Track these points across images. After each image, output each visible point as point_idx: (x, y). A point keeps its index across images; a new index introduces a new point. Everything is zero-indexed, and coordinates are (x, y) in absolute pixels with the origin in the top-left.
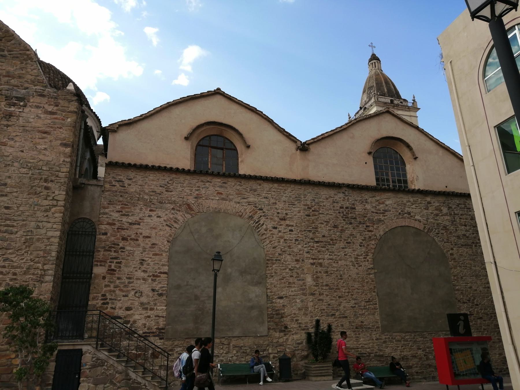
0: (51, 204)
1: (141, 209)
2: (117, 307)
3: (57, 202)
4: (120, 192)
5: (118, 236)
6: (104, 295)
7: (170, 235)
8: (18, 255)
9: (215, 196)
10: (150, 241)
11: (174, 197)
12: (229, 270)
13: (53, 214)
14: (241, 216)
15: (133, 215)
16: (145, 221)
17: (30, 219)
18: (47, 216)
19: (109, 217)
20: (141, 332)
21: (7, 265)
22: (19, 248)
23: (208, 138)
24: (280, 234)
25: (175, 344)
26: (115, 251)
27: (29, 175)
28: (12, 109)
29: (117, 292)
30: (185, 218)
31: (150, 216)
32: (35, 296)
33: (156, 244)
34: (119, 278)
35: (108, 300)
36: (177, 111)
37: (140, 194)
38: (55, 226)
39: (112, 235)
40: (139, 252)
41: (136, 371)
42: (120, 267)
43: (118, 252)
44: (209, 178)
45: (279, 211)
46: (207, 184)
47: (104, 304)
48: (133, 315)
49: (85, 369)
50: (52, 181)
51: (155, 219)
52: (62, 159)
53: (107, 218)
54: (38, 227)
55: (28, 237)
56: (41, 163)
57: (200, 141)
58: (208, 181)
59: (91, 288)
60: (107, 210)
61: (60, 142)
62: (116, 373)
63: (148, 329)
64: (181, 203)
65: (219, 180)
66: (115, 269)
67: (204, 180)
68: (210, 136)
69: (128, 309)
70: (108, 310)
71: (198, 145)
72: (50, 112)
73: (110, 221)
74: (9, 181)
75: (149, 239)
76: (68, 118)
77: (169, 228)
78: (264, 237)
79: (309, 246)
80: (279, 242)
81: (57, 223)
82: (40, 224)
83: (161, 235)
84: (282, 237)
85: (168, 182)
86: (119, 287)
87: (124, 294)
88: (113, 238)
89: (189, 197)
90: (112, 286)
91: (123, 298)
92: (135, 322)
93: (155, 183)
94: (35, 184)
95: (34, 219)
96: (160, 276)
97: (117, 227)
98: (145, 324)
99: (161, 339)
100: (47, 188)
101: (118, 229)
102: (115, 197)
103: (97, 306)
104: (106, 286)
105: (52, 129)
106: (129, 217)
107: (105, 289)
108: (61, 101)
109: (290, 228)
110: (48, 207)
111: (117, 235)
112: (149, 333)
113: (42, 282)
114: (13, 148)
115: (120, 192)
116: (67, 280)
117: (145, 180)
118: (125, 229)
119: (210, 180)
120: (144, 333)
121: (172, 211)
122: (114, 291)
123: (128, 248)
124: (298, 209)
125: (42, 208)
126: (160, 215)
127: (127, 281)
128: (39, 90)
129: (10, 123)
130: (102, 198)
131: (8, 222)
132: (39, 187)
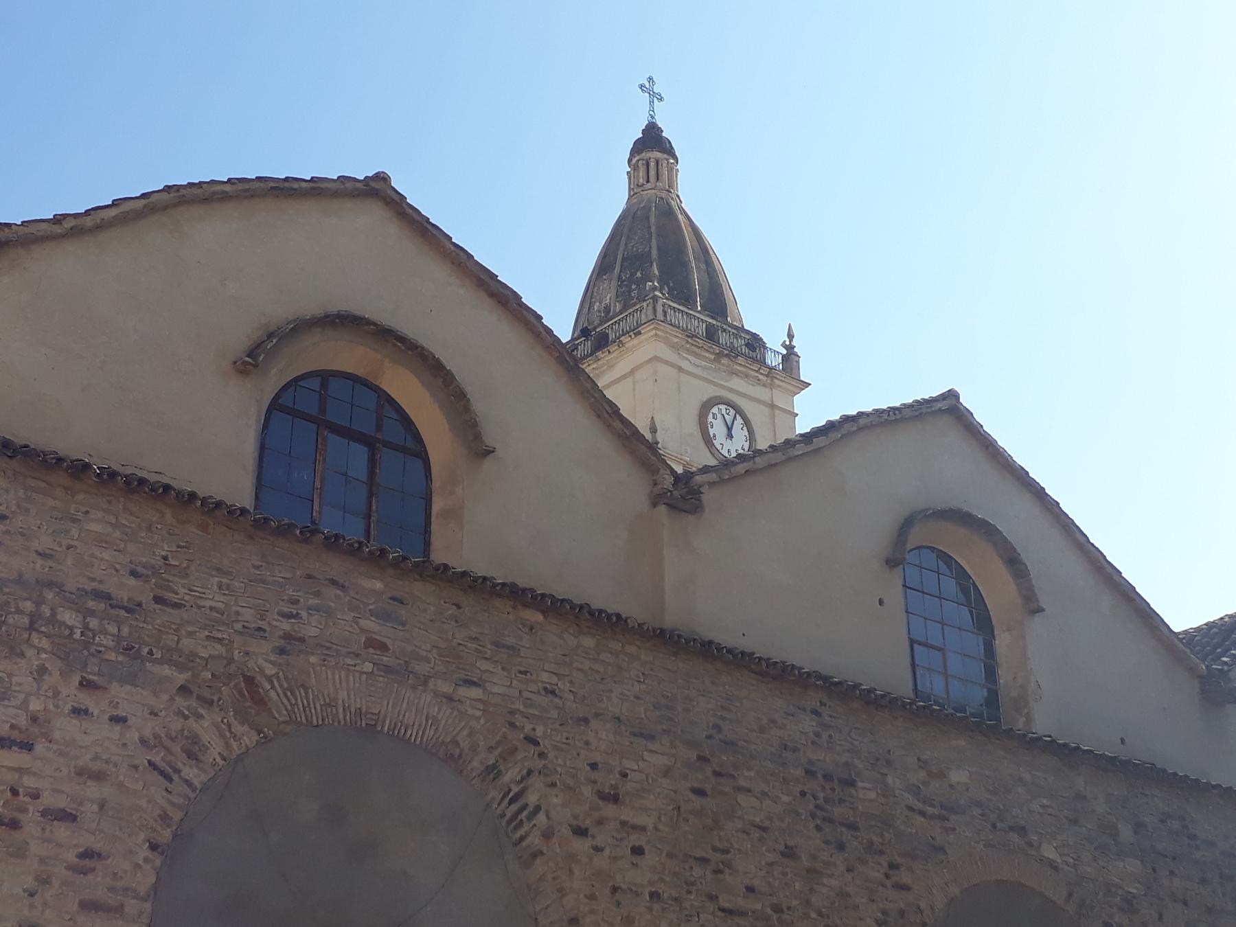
117: (67, 531)
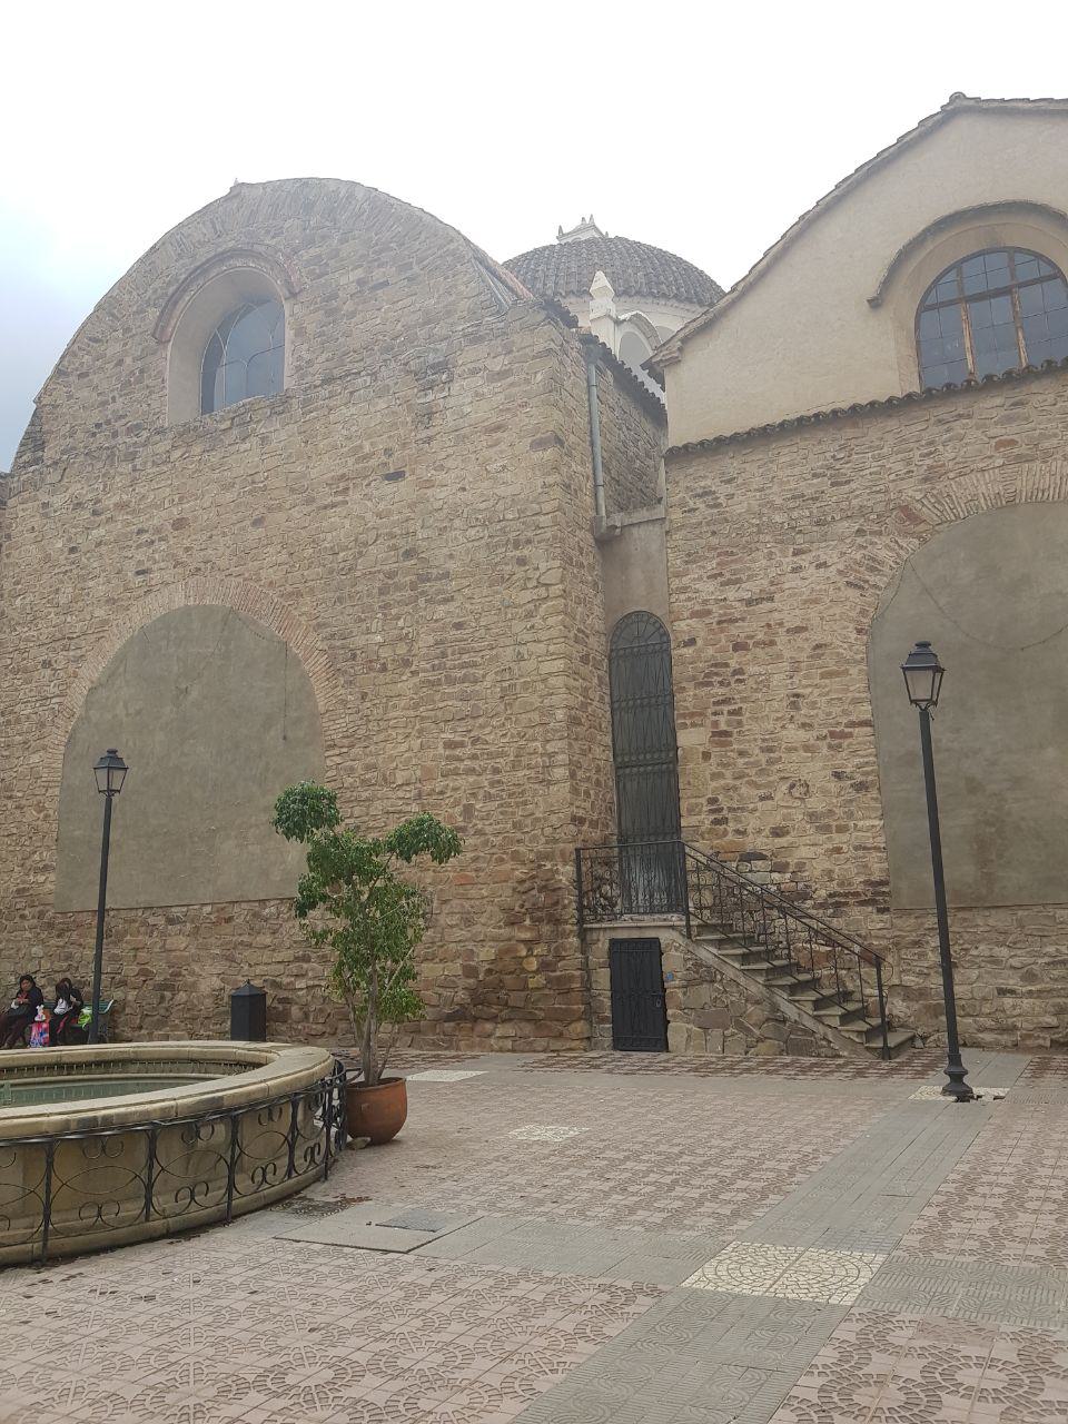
0: (535, 597)
1: (770, 556)
2: (750, 830)
3: (547, 590)
4: (708, 524)
6: (713, 801)
7: (863, 612)
9: (990, 457)
10: (807, 640)
11: (857, 496)
13: (544, 619)
15: (750, 578)
16: (786, 586)
17: (502, 641)
18: (533, 627)
20: (823, 893)
23: (952, 276)
25: (926, 926)
26: (721, 683)
27: (483, 541)
28: (430, 397)
29: (744, 790)
31: (795, 570)
33: (825, 645)
34: (742, 754)
36: (833, 228)
37: (761, 515)
38: (552, 648)
39: (707, 643)
40: (783, 676)
42: (740, 723)
43: (729, 684)
44: (961, 405)
46: (958, 427)
47: (716, 822)
48: (790, 847)
49: (673, 986)
50: (529, 542)
52: (540, 482)
53: (689, 599)
54: (520, 658)
55: (505, 684)
56: (500, 506)
58: (960, 416)
59: (681, 786)
60: (685, 580)
63: (841, 884)
64: (880, 508)
66: (729, 729)
67: (945, 417)
68: (957, 266)
69: (778, 832)
70: (730, 837)
71: (924, 308)
73: (697, 608)
74: (451, 566)
75: (803, 635)
77: (857, 592)
81: (555, 641)
82: (523, 649)
83: (837, 617)
85: (833, 457)
87: (762, 792)
88: (711, 651)
89: (903, 485)
90: (728, 774)
92: (801, 866)
93: (797, 471)
95: (509, 641)
96: (850, 735)
98: (830, 872)
99: (881, 911)
100: (522, 562)
101: (719, 623)
103: (703, 829)
104: (715, 776)
105: (509, 416)
106: (743, 585)
107: (714, 784)
108: (515, 337)
110: (531, 606)
111: (720, 641)
112: (846, 895)
113: (549, 783)
114: (445, 488)
115: (708, 524)
116: (628, 771)
118: (736, 621)
119: (966, 412)
120: (830, 895)
121: (860, 540)
122: (735, 788)
123: (752, 669)
126: (823, 558)
127: (763, 758)
128: (470, 330)
131: (465, 658)
132: (506, 564)
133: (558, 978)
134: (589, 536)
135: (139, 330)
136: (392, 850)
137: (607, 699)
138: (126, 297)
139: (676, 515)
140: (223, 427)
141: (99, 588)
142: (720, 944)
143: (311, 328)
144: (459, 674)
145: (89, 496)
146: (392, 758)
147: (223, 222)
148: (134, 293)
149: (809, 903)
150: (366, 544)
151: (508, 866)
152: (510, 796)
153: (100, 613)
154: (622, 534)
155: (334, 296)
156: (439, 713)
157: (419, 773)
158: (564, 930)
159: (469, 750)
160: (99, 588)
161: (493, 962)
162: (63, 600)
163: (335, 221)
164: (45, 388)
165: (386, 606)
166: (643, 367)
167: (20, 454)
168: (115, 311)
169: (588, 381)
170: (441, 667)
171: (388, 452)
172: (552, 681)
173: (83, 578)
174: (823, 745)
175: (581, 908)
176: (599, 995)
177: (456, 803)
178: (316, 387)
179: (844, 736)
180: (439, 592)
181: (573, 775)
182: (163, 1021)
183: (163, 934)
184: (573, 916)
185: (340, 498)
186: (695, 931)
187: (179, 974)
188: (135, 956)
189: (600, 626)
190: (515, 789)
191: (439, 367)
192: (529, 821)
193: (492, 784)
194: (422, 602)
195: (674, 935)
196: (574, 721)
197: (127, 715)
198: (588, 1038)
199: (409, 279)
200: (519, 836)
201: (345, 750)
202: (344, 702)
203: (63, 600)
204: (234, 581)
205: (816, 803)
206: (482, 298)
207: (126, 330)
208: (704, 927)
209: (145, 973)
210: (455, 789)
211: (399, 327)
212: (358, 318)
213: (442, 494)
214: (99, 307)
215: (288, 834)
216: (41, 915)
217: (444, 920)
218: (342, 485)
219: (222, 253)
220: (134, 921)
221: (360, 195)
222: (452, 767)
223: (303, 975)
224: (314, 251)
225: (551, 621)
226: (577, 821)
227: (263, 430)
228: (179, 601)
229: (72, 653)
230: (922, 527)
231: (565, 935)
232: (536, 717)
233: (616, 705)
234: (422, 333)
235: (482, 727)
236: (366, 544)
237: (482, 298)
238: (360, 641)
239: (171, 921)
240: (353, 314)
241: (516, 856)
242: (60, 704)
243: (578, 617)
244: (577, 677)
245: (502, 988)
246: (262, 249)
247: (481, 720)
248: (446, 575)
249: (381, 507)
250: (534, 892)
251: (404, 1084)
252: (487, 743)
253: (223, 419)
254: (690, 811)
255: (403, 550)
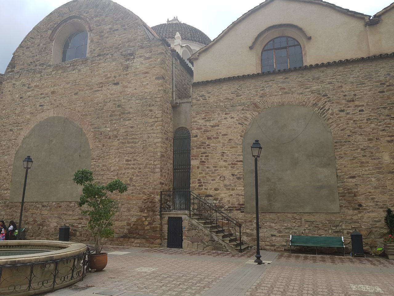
0: (154, 121)
1: (219, 114)
2: (209, 188)
4: (203, 104)
5: (205, 137)
6: (199, 180)
7: (243, 131)
8: (140, 156)
9: (278, 92)
10: (227, 138)
11: (243, 100)
12: (296, 155)
14: (304, 105)
15: (213, 120)
16: (223, 123)
17: (144, 132)
18: (153, 129)
19: (197, 123)
20: (227, 206)
21: (135, 163)
22: (140, 152)
23: (271, 42)
24: (348, 116)
25: (254, 217)
27: (140, 104)
28: (128, 62)
30: (253, 116)
31: (225, 119)
32: (152, 182)
34: (208, 167)
35: (202, 183)
36: (241, 26)
37: (217, 103)
38: (158, 135)
39: (201, 137)
41: (218, 235)
44: (271, 77)
45: (346, 93)
46: (270, 83)
47: (199, 186)
48: (220, 194)
50: (153, 105)
51: (229, 119)
54: (149, 137)
55: (144, 145)
56: (146, 95)
57: (265, 46)
59: (191, 176)
60: (196, 119)
61: (155, 77)
62: (204, 235)
64: (249, 103)
65: (281, 77)
67: (267, 80)
68: (273, 40)
69: (216, 189)
71: (264, 50)
72: (147, 58)
73: (198, 127)
74: (131, 110)
75: (226, 136)
76: (158, 59)
77: (241, 126)
78: (331, 121)
79: (385, 123)
80: (348, 124)
81: (159, 133)
82: (150, 135)
83: (235, 132)
84: (350, 119)
85: (237, 89)
86: (209, 174)
87: (212, 178)
88: (201, 139)
89: (255, 98)
90: (204, 173)
91: (212, 181)
92: (222, 199)
93: (227, 92)
94: (144, 109)
96: (237, 164)
97: (203, 131)
98: (229, 201)
99: (242, 212)
100: (151, 111)
101: (204, 131)
102: (200, 109)
104: (200, 173)
107: (200, 175)
108: (153, 48)
109: (360, 108)
112: (233, 207)
113: (155, 173)
115: (203, 104)
116: (177, 171)
118: (208, 131)
119: (272, 79)
120: (229, 207)
121: (243, 112)
122: (205, 177)
123: (212, 145)
124: (369, 87)
125: (150, 124)
126: (233, 116)
127: (213, 169)
128: (140, 45)
129: (127, 72)
130: (192, 111)
131: (133, 136)
132: (146, 111)
133: (153, 227)
134: (170, 105)
135: (45, 36)
136: (107, 189)
137: (172, 150)
138: (42, 26)
139: (194, 101)
140: (68, 66)
141: (28, 109)
142: (198, 219)
143: (95, 40)
144: (131, 141)
145: (27, 83)
146: (111, 163)
147: (72, 8)
148: (45, 26)
149: (223, 209)
150: (107, 103)
151: (141, 195)
152: (143, 176)
153: (28, 117)
154: (179, 105)
155: (103, 32)
156: (125, 151)
157: (118, 168)
158: (156, 214)
159: (132, 162)
160: (28, 109)
161: (135, 222)
162: (17, 112)
163: (104, 11)
164: (16, 50)
165: (112, 120)
166: (188, 59)
167: (7, 69)
168: (39, 30)
169: (172, 62)
170: (126, 138)
171: (115, 77)
172: (157, 144)
173: (24, 106)
174: (230, 166)
175: (161, 208)
176: (164, 232)
177: (128, 177)
178: (95, 57)
179: (235, 164)
180: (127, 117)
181: (161, 171)
182: (38, 236)
183: (41, 210)
184: (159, 210)
185: (100, 89)
186: (192, 215)
187: (45, 222)
188: (32, 216)
189: (171, 130)
190: (145, 174)
191: (131, 54)
192: (148, 183)
193: (138, 172)
194: (122, 119)
195: (186, 216)
196: (162, 156)
197: (34, 146)
198: (161, 244)
199: (124, 29)
200: (145, 187)
201: (96, 160)
202: (98, 147)
203: (17, 112)
204: (68, 110)
205: (227, 182)
206: (144, 36)
207: (42, 36)
208: (194, 214)
209: (35, 221)
210: (128, 173)
211: (120, 42)
212: (109, 38)
213: (130, 90)
214: (34, 29)
215: (77, 183)
216: (5, 203)
217: (122, 209)
218: (101, 85)
219: (71, 17)
220: (33, 206)
221: (112, 4)
222: (127, 167)
223: (81, 223)
224: (98, 19)
225: (158, 128)
226: (161, 184)
227: (79, 68)
228: (51, 114)
229: (19, 127)
230: (259, 109)
231: (156, 215)
232: (152, 154)
233: (175, 152)
234: (127, 45)
235: (136, 156)
236: (107, 103)
237: (144, 36)
238: (103, 130)
239: (43, 206)
240: (107, 37)
241: (144, 193)
242: (14, 142)
243: (166, 127)
244: (164, 144)
245: (137, 229)
246: (82, 17)
247: (136, 154)
248: (129, 113)
249: (112, 92)
250: (148, 203)
251: (107, 254)
252: (138, 161)
253: (68, 64)
254: (193, 183)
255: (117, 105)
